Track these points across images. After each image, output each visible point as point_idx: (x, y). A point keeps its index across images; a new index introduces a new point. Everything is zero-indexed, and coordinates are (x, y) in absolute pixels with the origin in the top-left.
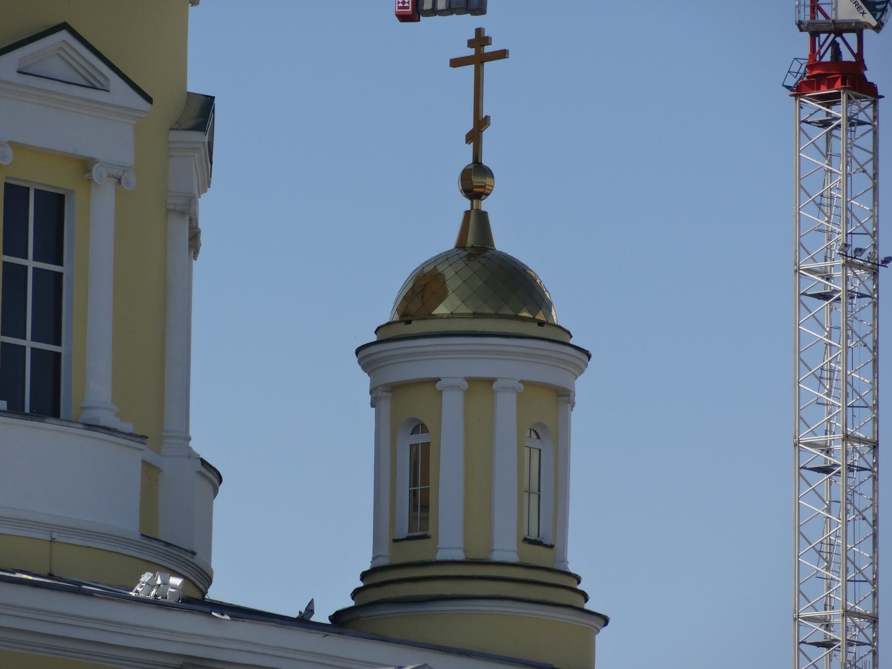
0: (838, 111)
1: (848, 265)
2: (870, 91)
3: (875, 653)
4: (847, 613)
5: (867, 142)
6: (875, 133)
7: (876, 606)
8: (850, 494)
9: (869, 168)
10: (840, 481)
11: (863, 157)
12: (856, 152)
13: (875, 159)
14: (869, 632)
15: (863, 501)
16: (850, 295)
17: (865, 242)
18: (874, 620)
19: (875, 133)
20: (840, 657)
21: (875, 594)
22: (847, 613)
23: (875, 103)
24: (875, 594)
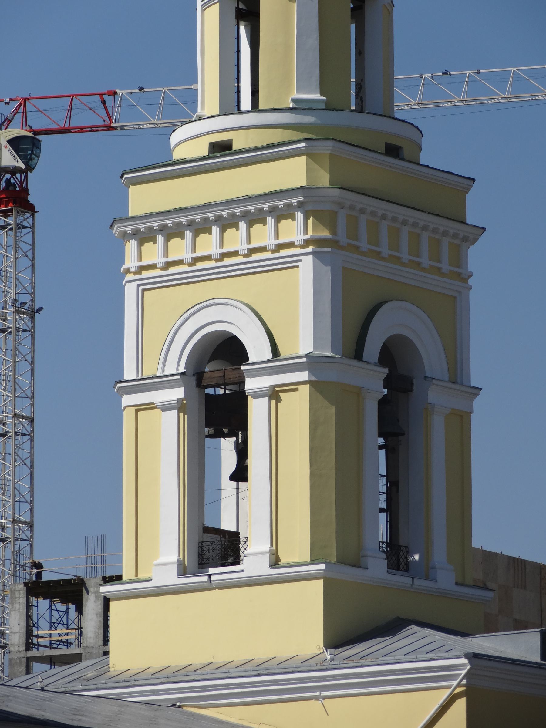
0: (11, 220)
1: (16, 312)
2: (30, 208)
3: (31, 546)
4: (15, 521)
5: (28, 238)
6: (33, 234)
7: (32, 517)
8: (17, 449)
9: (29, 254)
10: (11, 441)
11: (26, 248)
12: (21, 244)
13: (33, 249)
14: (28, 533)
15: (24, 454)
16: (18, 330)
17: (27, 299)
18: (31, 526)
19: (33, 234)
20: (10, 548)
21: (31, 510)
22: (15, 521)
23: (33, 216)
24: (31, 510)
